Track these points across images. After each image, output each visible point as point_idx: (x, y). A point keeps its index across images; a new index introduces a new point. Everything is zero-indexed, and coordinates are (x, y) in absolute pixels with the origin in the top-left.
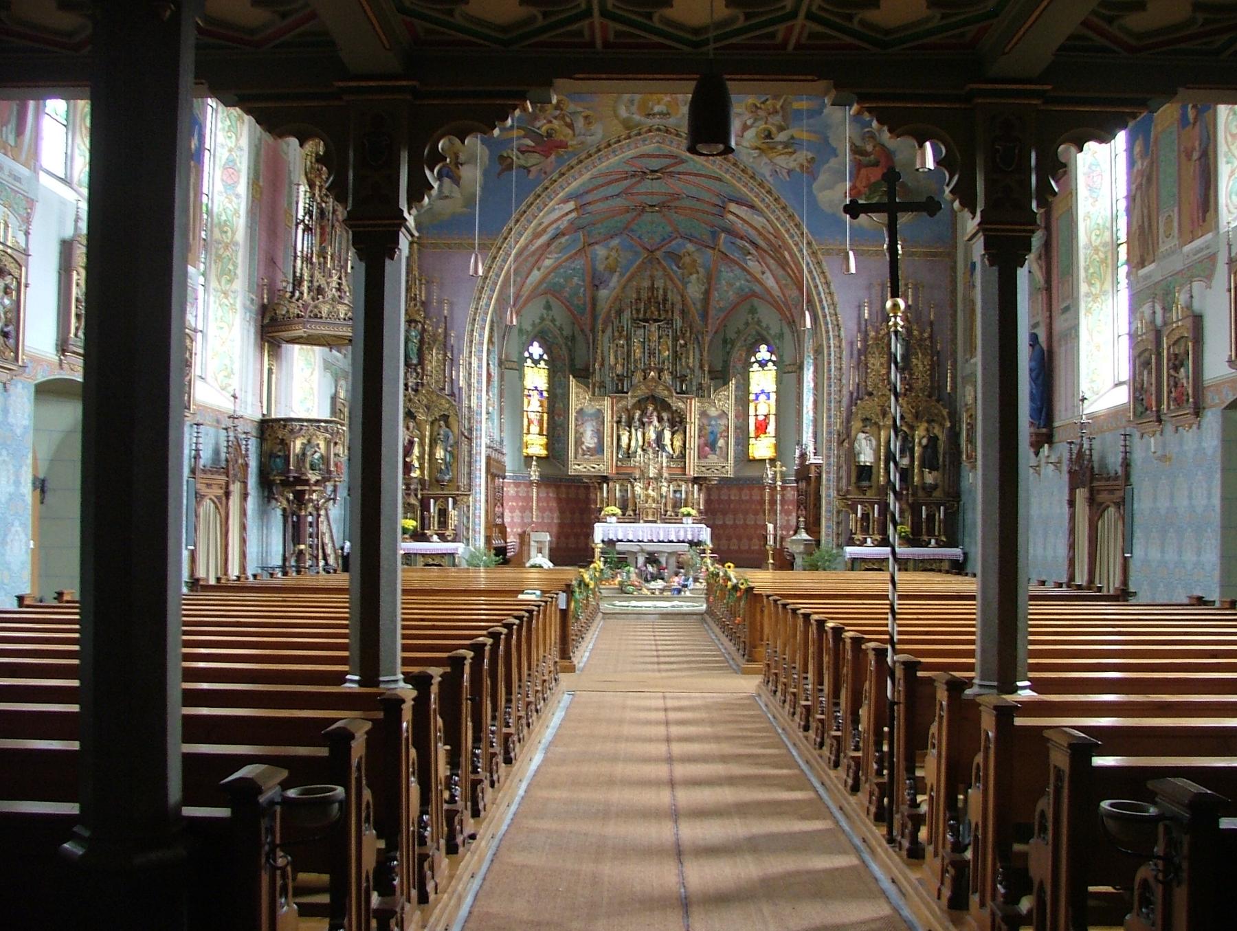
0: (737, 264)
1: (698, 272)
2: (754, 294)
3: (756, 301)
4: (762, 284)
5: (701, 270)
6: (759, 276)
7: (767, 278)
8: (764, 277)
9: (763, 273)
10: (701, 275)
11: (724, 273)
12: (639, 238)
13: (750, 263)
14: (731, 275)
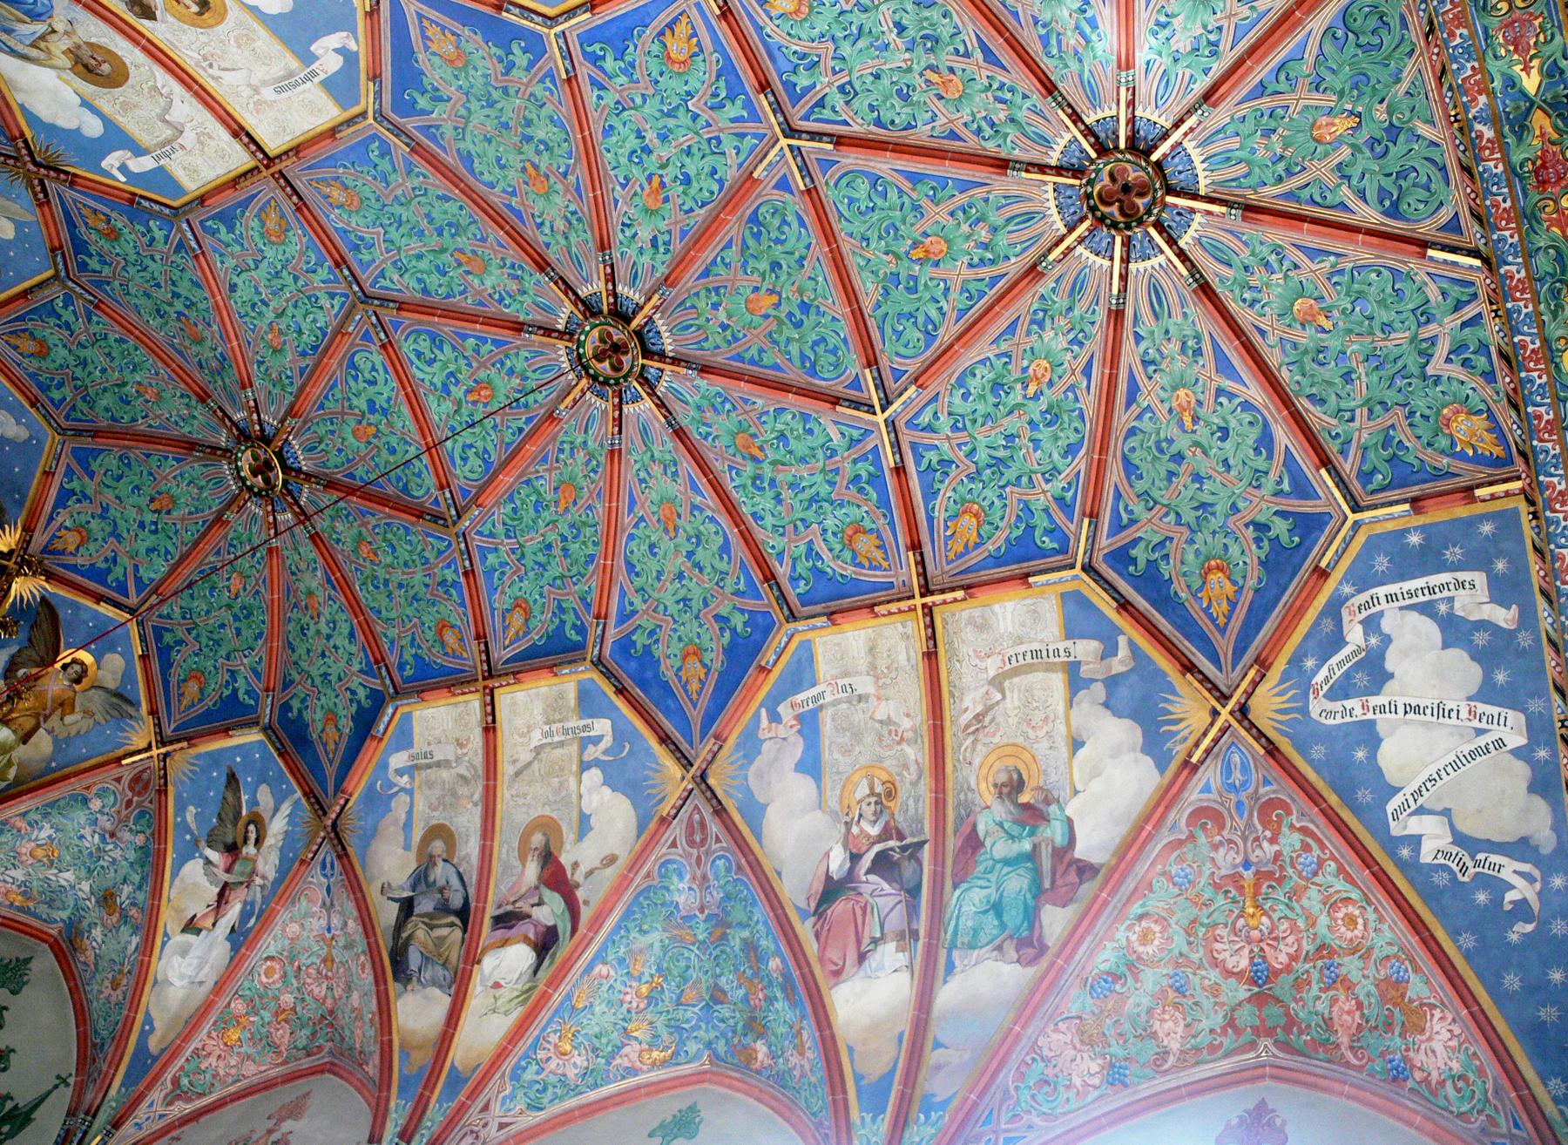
0: (159, 834)
1: (25, 739)
2: (66, 948)
3: (44, 963)
4: (147, 947)
5: (42, 743)
6: (169, 920)
7: (184, 952)
8: (179, 939)
9: (191, 927)
10: (22, 752)
11: (81, 816)
12: (65, 496)
13: (193, 869)
14: (92, 840)
